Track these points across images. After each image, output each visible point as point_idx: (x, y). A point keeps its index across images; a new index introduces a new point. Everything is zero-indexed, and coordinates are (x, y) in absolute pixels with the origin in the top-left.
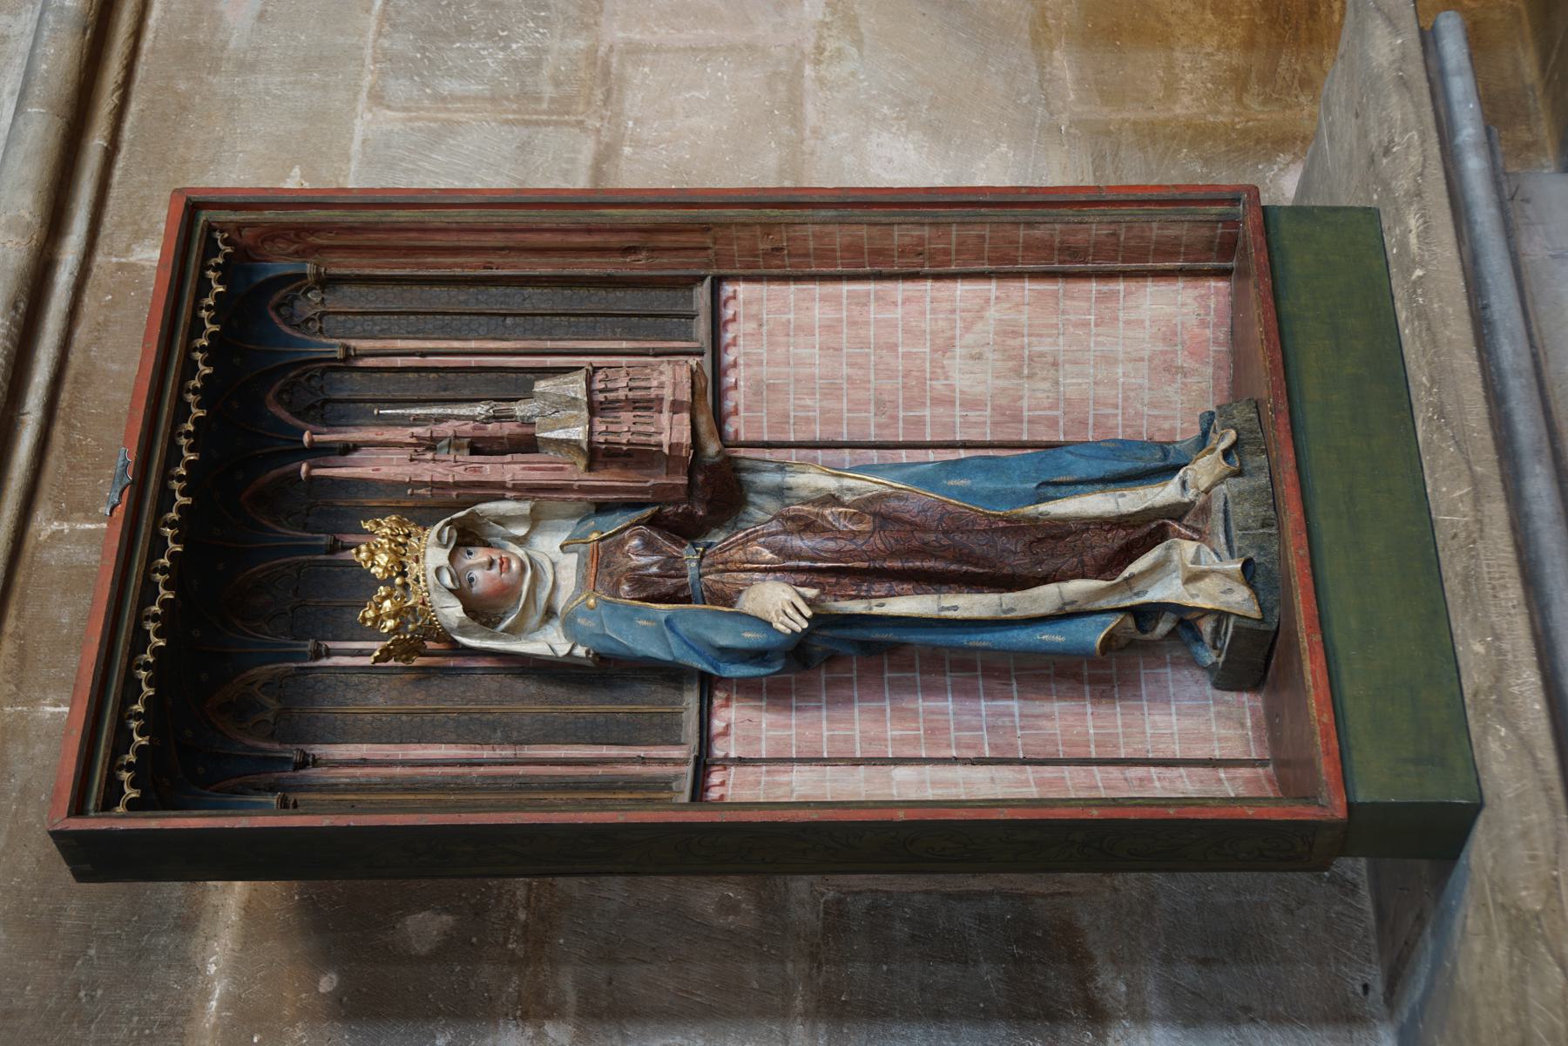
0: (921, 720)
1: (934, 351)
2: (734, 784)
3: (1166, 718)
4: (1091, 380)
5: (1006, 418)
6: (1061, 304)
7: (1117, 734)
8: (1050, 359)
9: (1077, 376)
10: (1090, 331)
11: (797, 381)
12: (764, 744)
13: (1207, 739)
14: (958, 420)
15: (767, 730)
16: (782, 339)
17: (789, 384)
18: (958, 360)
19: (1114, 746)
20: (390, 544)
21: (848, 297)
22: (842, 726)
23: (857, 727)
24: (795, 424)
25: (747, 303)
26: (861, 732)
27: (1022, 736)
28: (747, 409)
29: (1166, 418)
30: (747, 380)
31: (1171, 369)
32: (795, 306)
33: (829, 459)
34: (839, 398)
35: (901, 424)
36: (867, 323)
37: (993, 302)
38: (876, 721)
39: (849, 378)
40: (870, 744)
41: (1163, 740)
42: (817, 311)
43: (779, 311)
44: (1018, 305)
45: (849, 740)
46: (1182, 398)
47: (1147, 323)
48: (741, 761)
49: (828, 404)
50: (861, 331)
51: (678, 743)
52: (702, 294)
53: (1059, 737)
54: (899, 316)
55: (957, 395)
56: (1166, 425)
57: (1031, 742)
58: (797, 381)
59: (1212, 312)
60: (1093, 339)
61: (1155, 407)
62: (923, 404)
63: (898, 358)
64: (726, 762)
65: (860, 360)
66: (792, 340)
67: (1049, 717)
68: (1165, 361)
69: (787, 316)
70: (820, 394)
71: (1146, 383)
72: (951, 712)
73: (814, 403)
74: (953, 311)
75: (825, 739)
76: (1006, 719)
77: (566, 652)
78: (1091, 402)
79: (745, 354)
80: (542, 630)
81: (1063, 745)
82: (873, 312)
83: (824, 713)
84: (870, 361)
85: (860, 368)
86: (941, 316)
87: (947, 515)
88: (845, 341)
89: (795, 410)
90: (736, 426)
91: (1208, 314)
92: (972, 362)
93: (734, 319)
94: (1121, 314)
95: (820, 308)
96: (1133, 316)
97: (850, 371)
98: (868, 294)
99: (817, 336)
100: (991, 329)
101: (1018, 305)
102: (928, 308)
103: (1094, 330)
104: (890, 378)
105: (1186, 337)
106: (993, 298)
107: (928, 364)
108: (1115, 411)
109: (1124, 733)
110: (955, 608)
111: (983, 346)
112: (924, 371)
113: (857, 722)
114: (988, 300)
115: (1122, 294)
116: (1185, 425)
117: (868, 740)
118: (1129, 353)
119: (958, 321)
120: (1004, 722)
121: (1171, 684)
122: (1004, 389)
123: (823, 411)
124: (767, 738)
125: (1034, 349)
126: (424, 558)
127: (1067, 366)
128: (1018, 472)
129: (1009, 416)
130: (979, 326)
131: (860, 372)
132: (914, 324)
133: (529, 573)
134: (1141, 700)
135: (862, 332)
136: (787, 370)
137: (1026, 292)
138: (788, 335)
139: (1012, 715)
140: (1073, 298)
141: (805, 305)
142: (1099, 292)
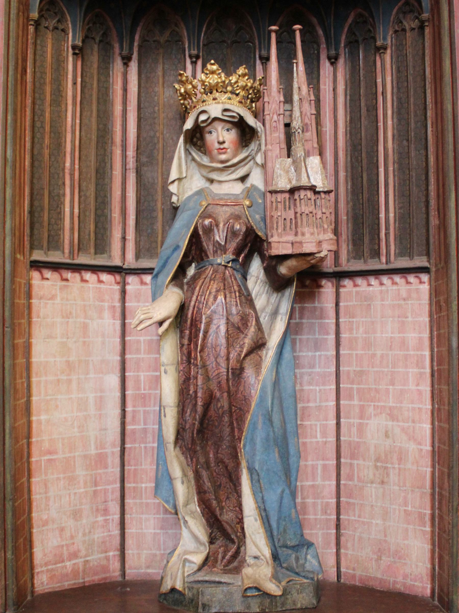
1: (390, 408)
4: (374, 503)
6: (417, 490)
7: (142, 499)
8: (386, 480)
14: (352, 421)
18: (385, 423)
22: (147, 348)
26: (143, 358)
27: (141, 447)
29: (353, 545)
35: (349, 386)
36: (406, 367)
37: (419, 447)
38: (150, 367)
44: (417, 462)
45: (138, 351)
47: (406, 542)
48: (124, 292)
51: (137, 257)
53: (139, 467)
55: (366, 421)
59: (412, 583)
60: (397, 507)
61: (359, 540)
62: (360, 400)
64: (124, 284)
68: (384, 550)
71: (373, 537)
74: (413, 421)
75: (138, 338)
78: (362, 502)
80: (202, 178)
81: (135, 469)
85: (380, 362)
86: (411, 414)
87: (242, 413)
90: (348, 286)
91: (411, 580)
101: (417, 462)
103: (403, 508)
106: (422, 447)
107: (382, 404)
108: (357, 515)
109: (142, 503)
113: (149, 356)
114: (420, 444)
115: (424, 529)
117: (138, 362)
121: (174, 531)
123: (356, 339)
125: (391, 470)
127: (381, 490)
132: (406, 396)
133: (220, 166)
137: (425, 469)
140: (421, 498)
142: (425, 514)
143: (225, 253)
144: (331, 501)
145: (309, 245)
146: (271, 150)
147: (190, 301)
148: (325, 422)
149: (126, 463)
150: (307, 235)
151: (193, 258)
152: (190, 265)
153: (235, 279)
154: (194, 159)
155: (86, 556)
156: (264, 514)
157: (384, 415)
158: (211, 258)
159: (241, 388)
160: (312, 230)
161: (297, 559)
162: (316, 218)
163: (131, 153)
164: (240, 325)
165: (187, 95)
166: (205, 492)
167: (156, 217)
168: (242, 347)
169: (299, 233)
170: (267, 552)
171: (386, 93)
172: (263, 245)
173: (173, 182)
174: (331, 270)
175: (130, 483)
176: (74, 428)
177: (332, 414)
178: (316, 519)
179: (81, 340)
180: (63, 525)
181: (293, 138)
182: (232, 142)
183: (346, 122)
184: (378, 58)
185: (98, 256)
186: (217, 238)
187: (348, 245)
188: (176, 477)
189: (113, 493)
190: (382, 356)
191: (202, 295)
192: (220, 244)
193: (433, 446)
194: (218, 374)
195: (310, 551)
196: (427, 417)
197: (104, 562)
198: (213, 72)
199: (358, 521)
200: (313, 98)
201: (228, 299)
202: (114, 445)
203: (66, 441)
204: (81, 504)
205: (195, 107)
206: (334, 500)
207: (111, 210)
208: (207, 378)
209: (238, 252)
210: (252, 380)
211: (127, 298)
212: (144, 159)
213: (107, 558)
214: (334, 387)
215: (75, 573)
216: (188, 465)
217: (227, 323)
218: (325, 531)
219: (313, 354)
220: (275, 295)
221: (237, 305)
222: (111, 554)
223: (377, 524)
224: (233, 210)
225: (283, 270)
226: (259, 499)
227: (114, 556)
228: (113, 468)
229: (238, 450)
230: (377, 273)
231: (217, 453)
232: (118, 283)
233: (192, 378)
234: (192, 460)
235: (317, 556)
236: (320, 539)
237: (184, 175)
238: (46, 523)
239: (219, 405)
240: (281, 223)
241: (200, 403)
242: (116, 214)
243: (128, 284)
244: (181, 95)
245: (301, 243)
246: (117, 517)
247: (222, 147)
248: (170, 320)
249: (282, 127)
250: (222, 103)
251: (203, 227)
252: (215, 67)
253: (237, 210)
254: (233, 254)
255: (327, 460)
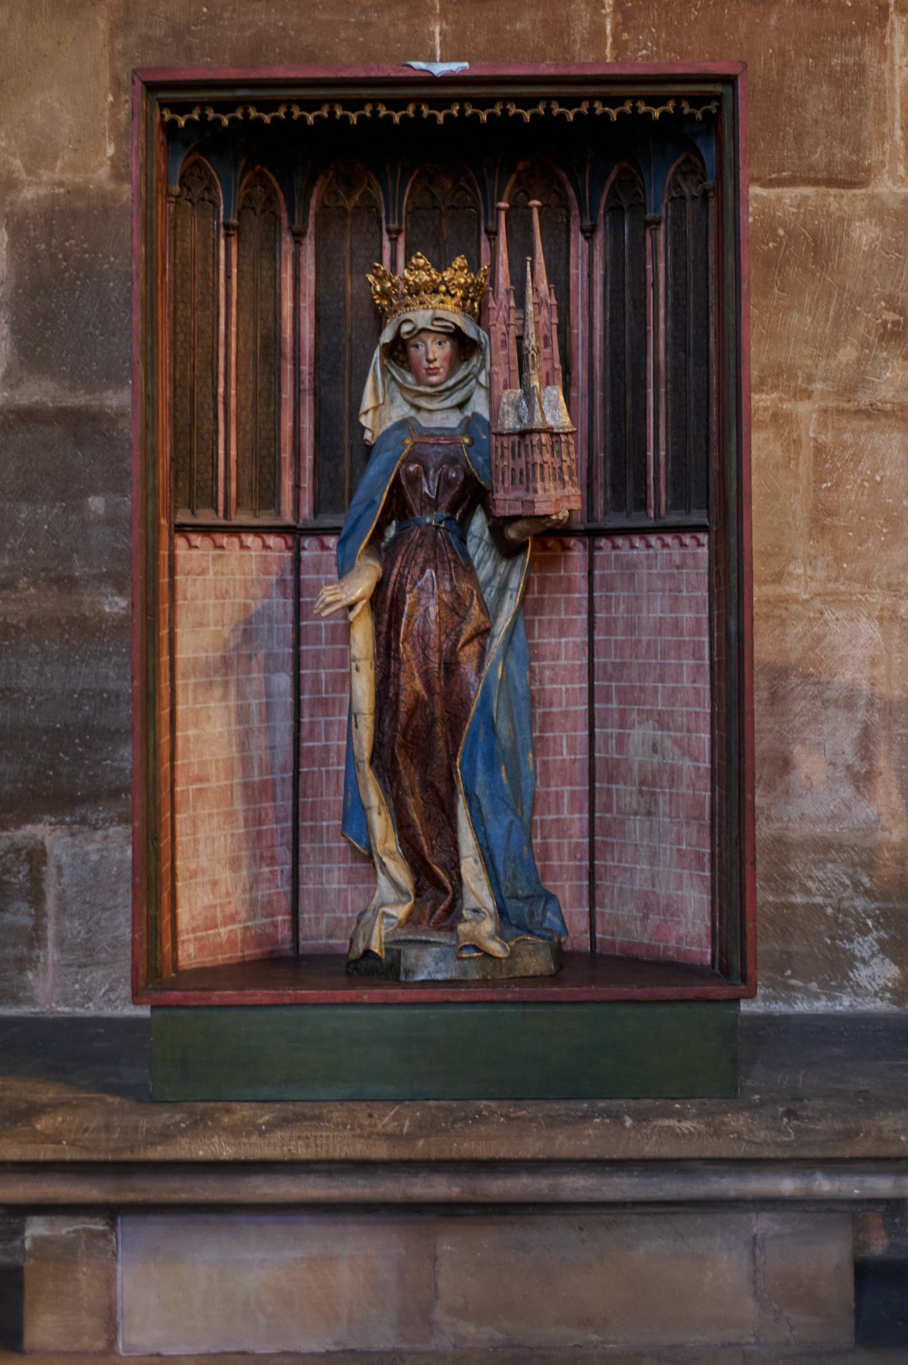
1: (659, 713)
4: (638, 842)
8: (653, 810)
9: (641, 831)
11: (637, 598)
14: (609, 730)
17: (634, 591)
18: (652, 732)
21: (699, 642)
34: (624, 634)
35: (606, 683)
36: (679, 657)
37: (695, 764)
47: (680, 893)
55: (628, 731)
59: (688, 948)
60: (668, 846)
62: (620, 703)
65: (652, 651)
66: (667, 594)
73: (620, 612)
74: (689, 730)
78: (622, 841)
82: (688, 662)
84: (651, 659)
85: (646, 651)
86: (685, 720)
89: (616, 596)
91: (687, 944)
92: (651, 744)
94: (686, 871)
96: (685, 881)
97: (644, 643)
98: (702, 658)
100: (675, 762)
103: (675, 847)
104: (640, 675)
105: (670, 924)
106: (699, 764)
107: (649, 707)
112: (644, 704)
114: (697, 760)
115: (702, 873)
118: (658, 875)
123: (615, 620)
125: (661, 797)
130: (678, 752)
131: (643, 651)
135: (672, 653)
136: (645, 589)
137: (703, 793)
142: (704, 854)
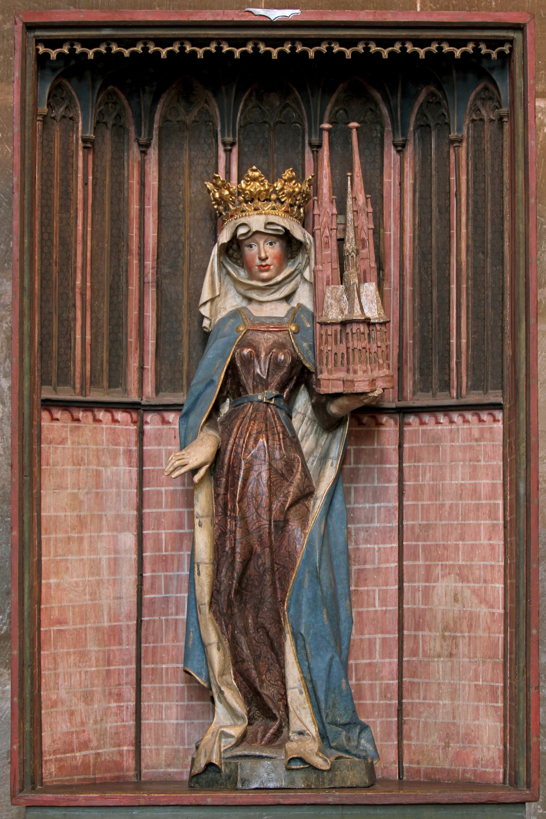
0: (173, 553)
1: (460, 567)
2: (115, 429)
3: (174, 716)
4: (441, 681)
5: (417, 620)
6: (489, 660)
8: (454, 652)
9: (444, 671)
10: (472, 681)
11: (441, 467)
12: (156, 447)
13: (157, 741)
14: (416, 584)
15: (166, 450)
16: (468, 458)
17: (439, 461)
18: (454, 585)
19: (152, 681)
20: (264, 191)
21: (494, 504)
22: (169, 500)
23: (168, 510)
24: (415, 466)
25: (491, 429)
26: (164, 512)
28: (423, 431)
29: (418, 733)
30: (442, 430)
31: (447, 739)
32: (489, 465)
33: (390, 492)
34: (430, 499)
37: (491, 610)
39: (442, 506)
40: (155, 519)
41: (157, 712)
42: (485, 481)
43: (486, 453)
44: (489, 628)
46: (430, 746)
47: (477, 722)
48: (141, 433)
49: (427, 490)
50: (472, 514)
51: (158, 390)
52: (495, 397)
53: (159, 644)
54: (482, 542)
56: (413, 734)
57: (156, 625)
58: (441, 467)
60: (467, 683)
61: (424, 727)
62: (426, 559)
63: (456, 541)
64: (141, 424)
65: (454, 513)
66: (467, 463)
67: (176, 638)
68: (453, 735)
69: (482, 460)
70: (433, 485)
71: (439, 720)
72: (179, 573)
73: (427, 480)
74: (485, 581)
75: (159, 488)
76: (174, 610)
77: (203, 313)
78: (427, 681)
79: (458, 429)
80: (238, 295)
81: (154, 647)
83: (180, 488)
84: (454, 520)
86: (482, 573)
88: (466, 502)
89: (422, 466)
92: (452, 595)
93: (481, 421)
94: (482, 704)
95: (487, 484)
97: (447, 507)
98: (497, 519)
99: (470, 482)
102: (487, 563)
104: (443, 535)
105: (467, 750)
106: (494, 611)
107: (451, 563)
108: (421, 697)
109: (162, 687)
110: (199, 574)
111: (462, 603)
112: (447, 560)
114: (492, 607)
115: (496, 705)
116: (413, 747)
118: (458, 709)
119: (478, 585)
120: (171, 608)
121: (201, 721)
122: (435, 618)
124: (160, 450)
125: (461, 640)
126: (257, 214)
127: (450, 664)
128: (313, 620)
129: (419, 621)
130: (476, 601)
131: (447, 514)
133: (261, 284)
134: (188, 701)
135: (472, 515)
136: (448, 460)
137: (497, 635)
138: (470, 461)
139: (177, 614)
140: (493, 669)
141: (490, 473)
142: (497, 688)
143: (267, 389)
144: (391, 682)
145: (362, 384)
146: (322, 271)
147: (227, 445)
148: (384, 588)
149: (143, 640)
150: (360, 373)
151: (228, 393)
152: (225, 401)
153: (279, 418)
154: (228, 273)
155: (98, 747)
156: (310, 686)
157: (453, 575)
158: (251, 394)
159: (285, 543)
160: (364, 368)
161: (349, 739)
162: (370, 353)
163: (150, 263)
164: (284, 471)
165: (222, 201)
166: (243, 661)
167: (181, 341)
168: (286, 496)
169: (351, 371)
170: (313, 730)
171: (460, 195)
172: (311, 377)
173: (205, 303)
174: (393, 405)
175: (148, 664)
176: (85, 595)
177: (394, 577)
178: (373, 705)
179: (94, 490)
180: (73, 708)
181: (346, 262)
182: (275, 257)
183: (414, 224)
184: (452, 151)
185: (112, 389)
186: (258, 371)
187: (414, 375)
188: (212, 642)
189: (127, 675)
190: (451, 507)
191: (240, 438)
192: (261, 378)
193: (505, 608)
194: (259, 527)
195: (363, 735)
196: (499, 575)
197: (117, 758)
198: (255, 179)
199: (423, 703)
200: (370, 210)
201: (270, 442)
202: (129, 618)
203: (77, 610)
204: (93, 685)
205: (232, 216)
206: (396, 682)
207: (127, 334)
208: (247, 532)
209: (282, 387)
210: (298, 533)
211: (145, 439)
212: (166, 270)
213: (121, 753)
214: (396, 545)
215: (85, 766)
216: (223, 633)
217: (270, 470)
218: (384, 719)
219: (371, 505)
220: (325, 436)
221: (280, 449)
222: (125, 748)
223: (445, 705)
224: (276, 337)
225: (333, 409)
226: (305, 669)
227: (128, 751)
228: (128, 645)
229: (281, 614)
230: (446, 409)
231: (257, 617)
232: (134, 422)
233: (228, 533)
234: (227, 627)
235: (372, 741)
236: (378, 729)
237: (218, 294)
238: (54, 704)
239: (260, 562)
240: (331, 358)
241: (238, 559)
242: (133, 339)
243: (147, 423)
244: (215, 199)
245: (352, 381)
246: (132, 704)
247: (264, 264)
248: (207, 466)
249: (334, 244)
250: (265, 214)
251: (242, 357)
252: (257, 174)
253: (281, 337)
254: (276, 389)
255: (388, 632)
